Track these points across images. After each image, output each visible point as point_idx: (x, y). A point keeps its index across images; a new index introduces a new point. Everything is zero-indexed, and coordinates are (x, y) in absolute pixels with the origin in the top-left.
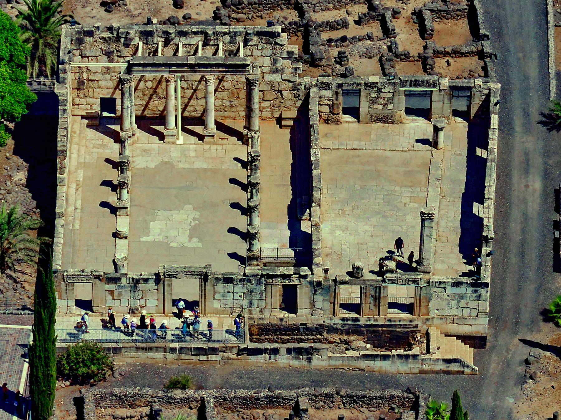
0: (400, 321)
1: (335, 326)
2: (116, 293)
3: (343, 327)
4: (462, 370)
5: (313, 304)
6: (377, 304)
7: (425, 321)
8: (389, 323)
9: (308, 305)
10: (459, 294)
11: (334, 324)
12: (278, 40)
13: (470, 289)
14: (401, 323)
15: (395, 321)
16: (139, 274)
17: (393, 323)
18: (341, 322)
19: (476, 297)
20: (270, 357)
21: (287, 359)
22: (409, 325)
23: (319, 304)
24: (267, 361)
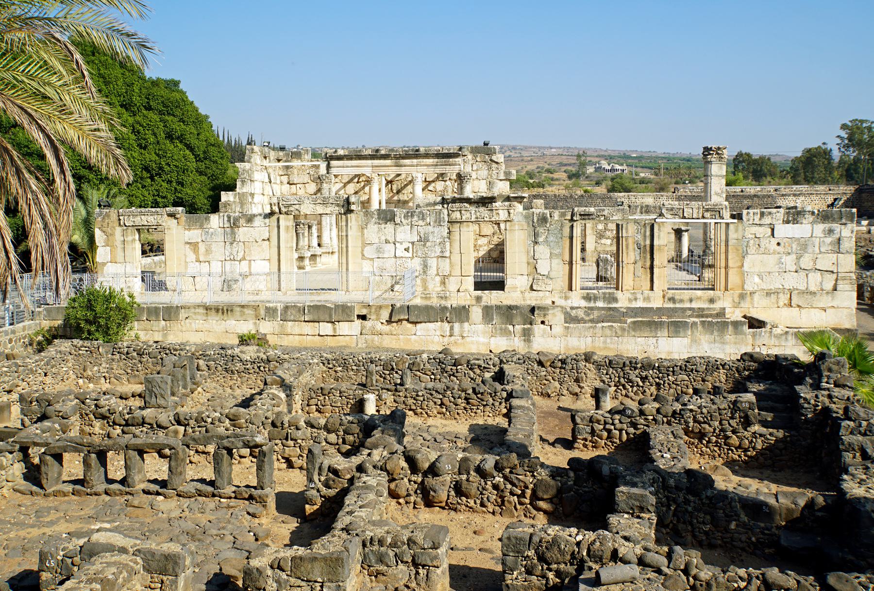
0: (691, 301)
2: (202, 248)
3: (588, 315)
6: (648, 264)
7: (737, 300)
8: (671, 305)
9: (525, 270)
10: (798, 239)
11: (572, 308)
12: (494, 158)
13: (820, 228)
14: (694, 305)
15: (681, 301)
17: (678, 305)
18: (584, 304)
19: (831, 243)
20: (452, 328)
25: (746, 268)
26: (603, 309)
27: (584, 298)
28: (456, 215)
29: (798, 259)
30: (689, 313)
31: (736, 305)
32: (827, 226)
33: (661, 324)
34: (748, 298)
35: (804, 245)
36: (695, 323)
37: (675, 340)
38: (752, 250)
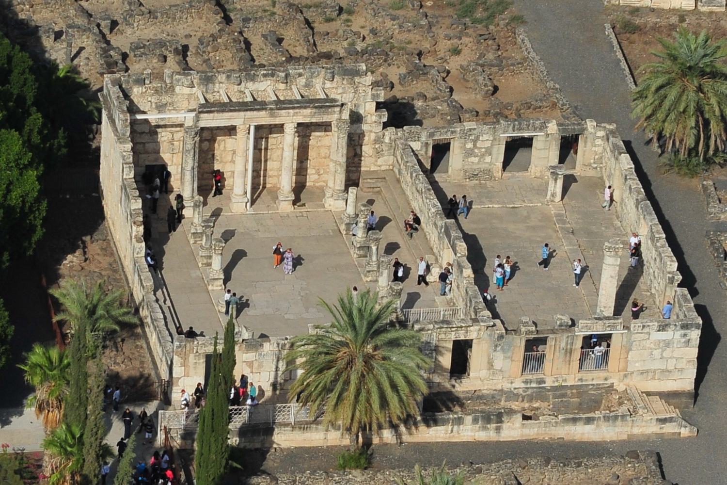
0: (593, 379)
1: (515, 391)
2: (256, 365)
3: (526, 392)
4: (678, 431)
5: (491, 365)
8: (580, 383)
10: (665, 340)
11: (515, 389)
14: (594, 382)
16: (284, 338)
17: (584, 383)
18: (523, 385)
19: (684, 342)
21: (472, 430)
22: (603, 384)
23: (498, 364)
24: (448, 435)
25: (629, 358)
26: (535, 388)
27: (523, 382)
28: (442, 336)
29: (663, 351)
30: (591, 387)
31: (621, 381)
32: (683, 332)
33: (580, 419)
34: (629, 376)
35: (668, 344)
36: (599, 417)
37: (586, 426)
38: (634, 348)
